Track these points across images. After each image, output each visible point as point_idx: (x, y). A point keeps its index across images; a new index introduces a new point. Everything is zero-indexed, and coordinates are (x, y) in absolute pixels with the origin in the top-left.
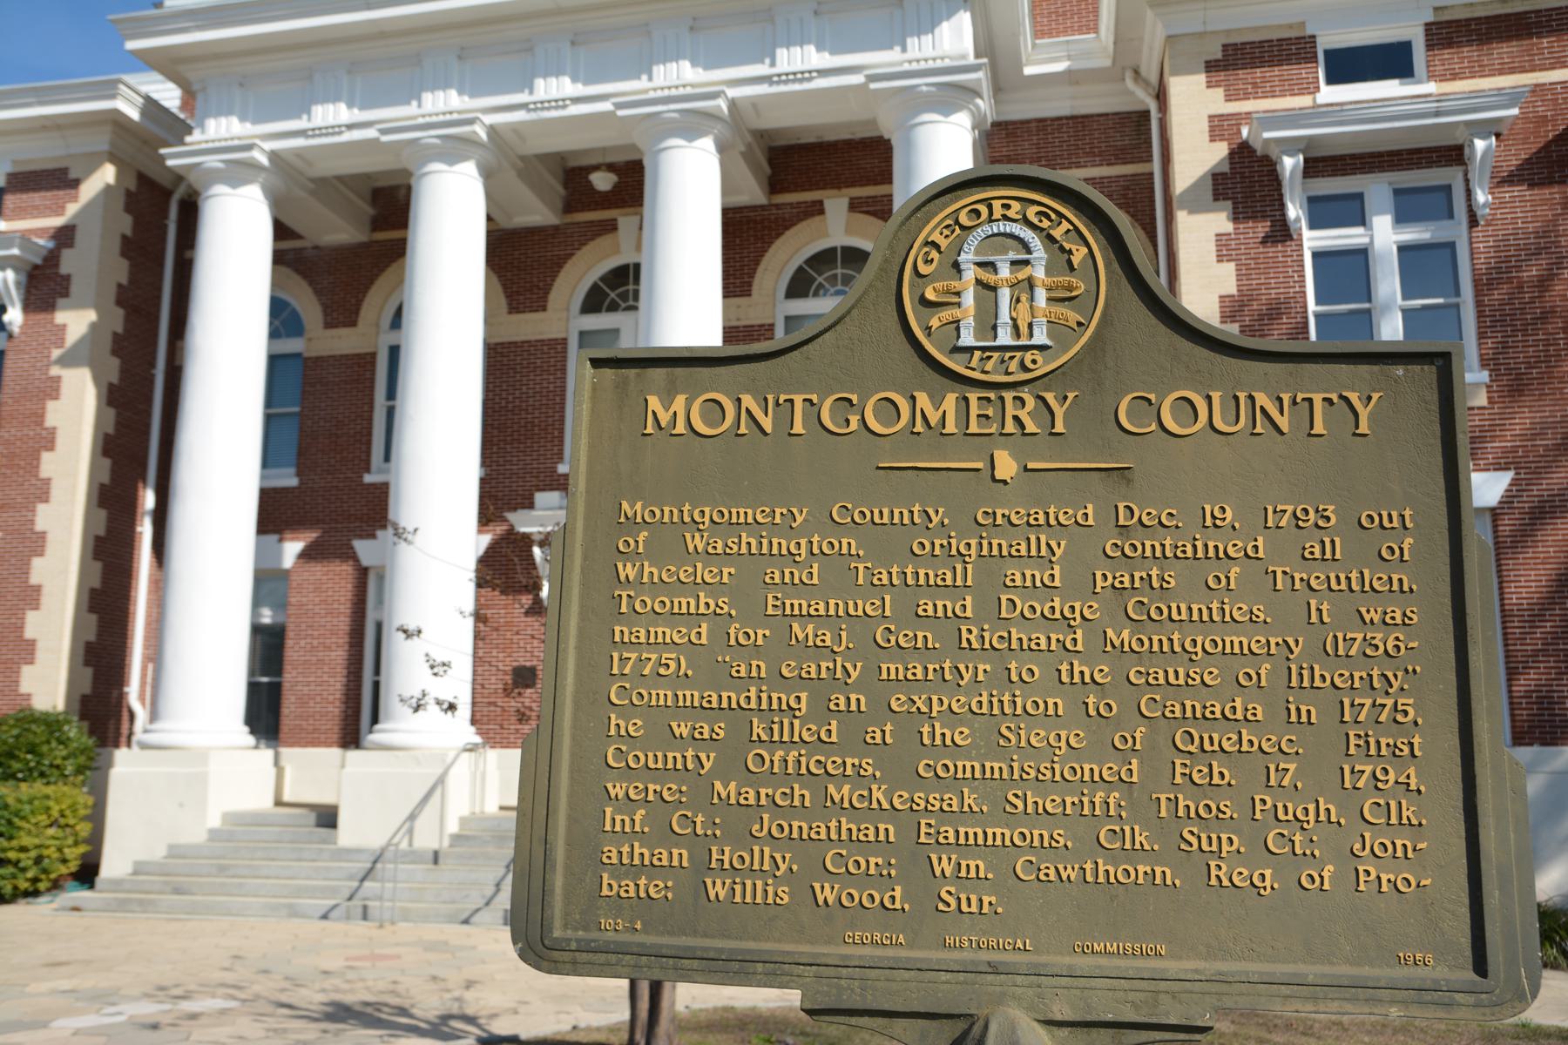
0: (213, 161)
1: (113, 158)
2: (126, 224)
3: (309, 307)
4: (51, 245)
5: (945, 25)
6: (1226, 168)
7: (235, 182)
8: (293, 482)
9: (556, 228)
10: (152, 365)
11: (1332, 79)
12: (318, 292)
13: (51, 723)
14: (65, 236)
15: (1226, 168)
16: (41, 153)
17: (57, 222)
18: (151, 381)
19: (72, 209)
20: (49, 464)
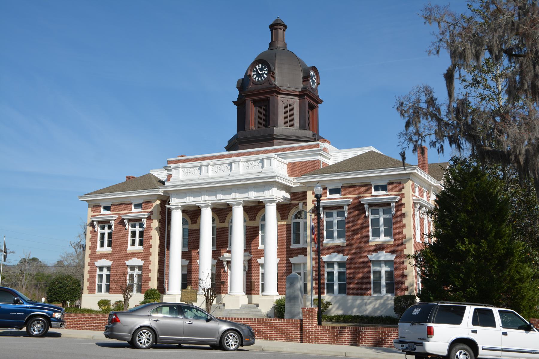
0: (173, 207)
1: (158, 199)
2: (160, 209)
3: (189, 221)
4: (149, 214)
5: (270, 190)
6: (314, 208)
7: (177, 210)
8: (188, 250)
9: (226, 208)
10: (165, 231)
11: (331, 193)
12: (190, 218)
13: (154, 290)
14: (151, 213)
15: (314, 208)
16: (148, 199)
17: (150, 210)
18: (165, 234)
19: (152, 208)
20: (151, 250)
